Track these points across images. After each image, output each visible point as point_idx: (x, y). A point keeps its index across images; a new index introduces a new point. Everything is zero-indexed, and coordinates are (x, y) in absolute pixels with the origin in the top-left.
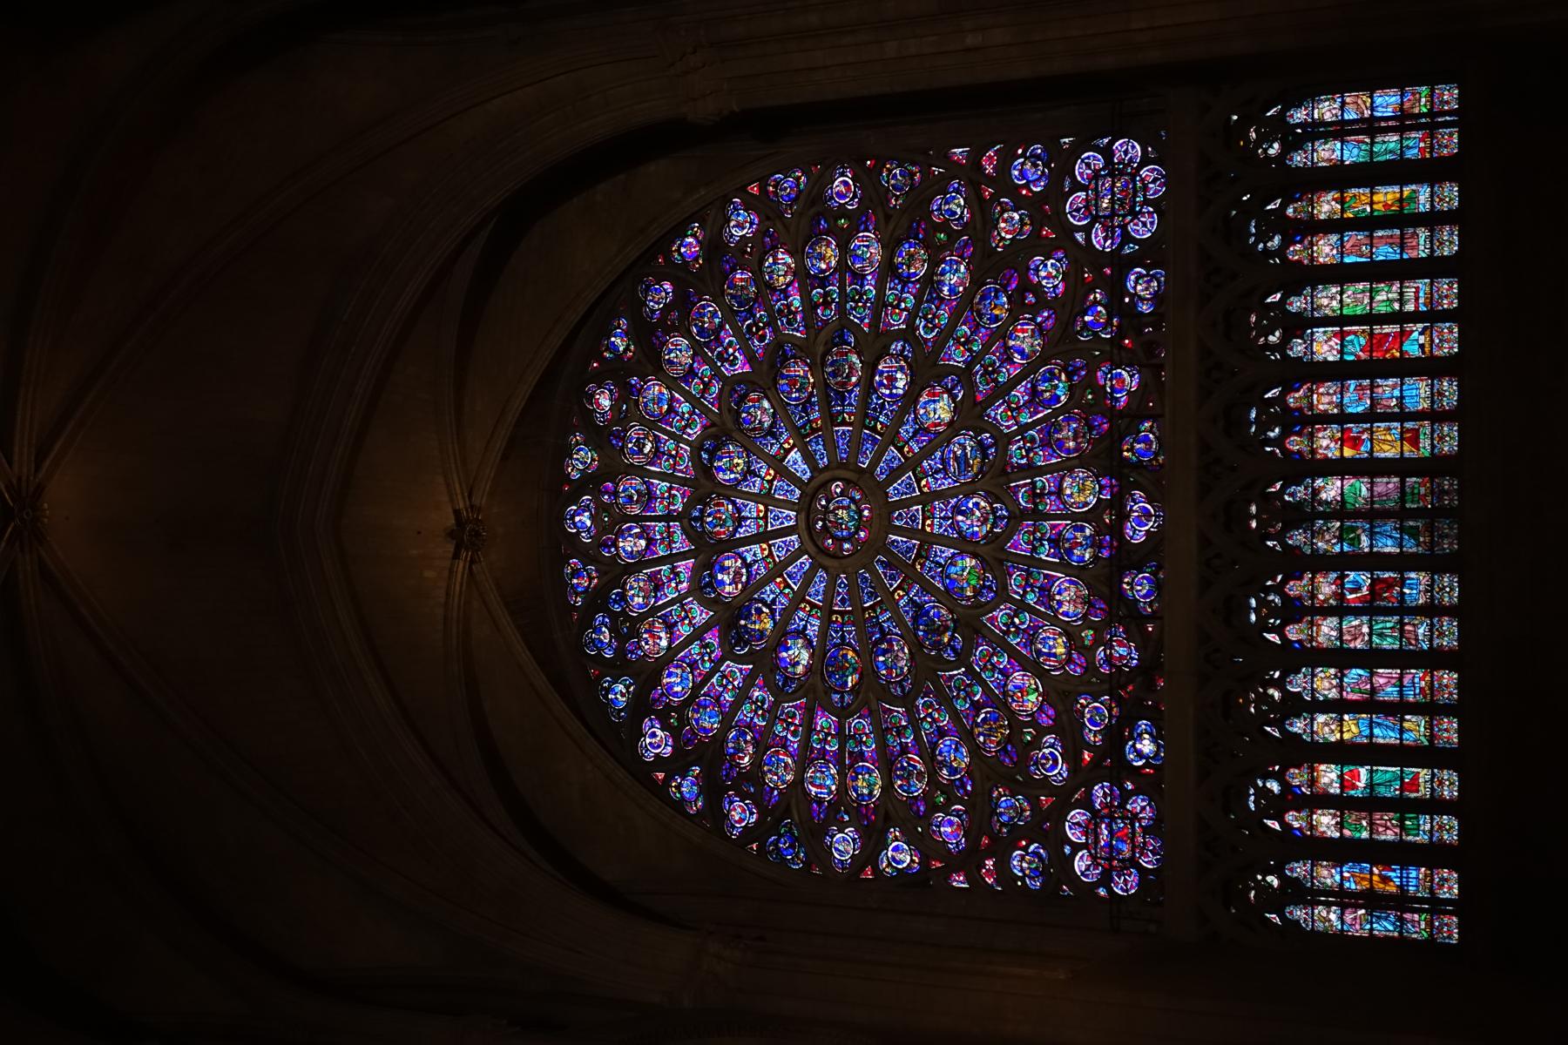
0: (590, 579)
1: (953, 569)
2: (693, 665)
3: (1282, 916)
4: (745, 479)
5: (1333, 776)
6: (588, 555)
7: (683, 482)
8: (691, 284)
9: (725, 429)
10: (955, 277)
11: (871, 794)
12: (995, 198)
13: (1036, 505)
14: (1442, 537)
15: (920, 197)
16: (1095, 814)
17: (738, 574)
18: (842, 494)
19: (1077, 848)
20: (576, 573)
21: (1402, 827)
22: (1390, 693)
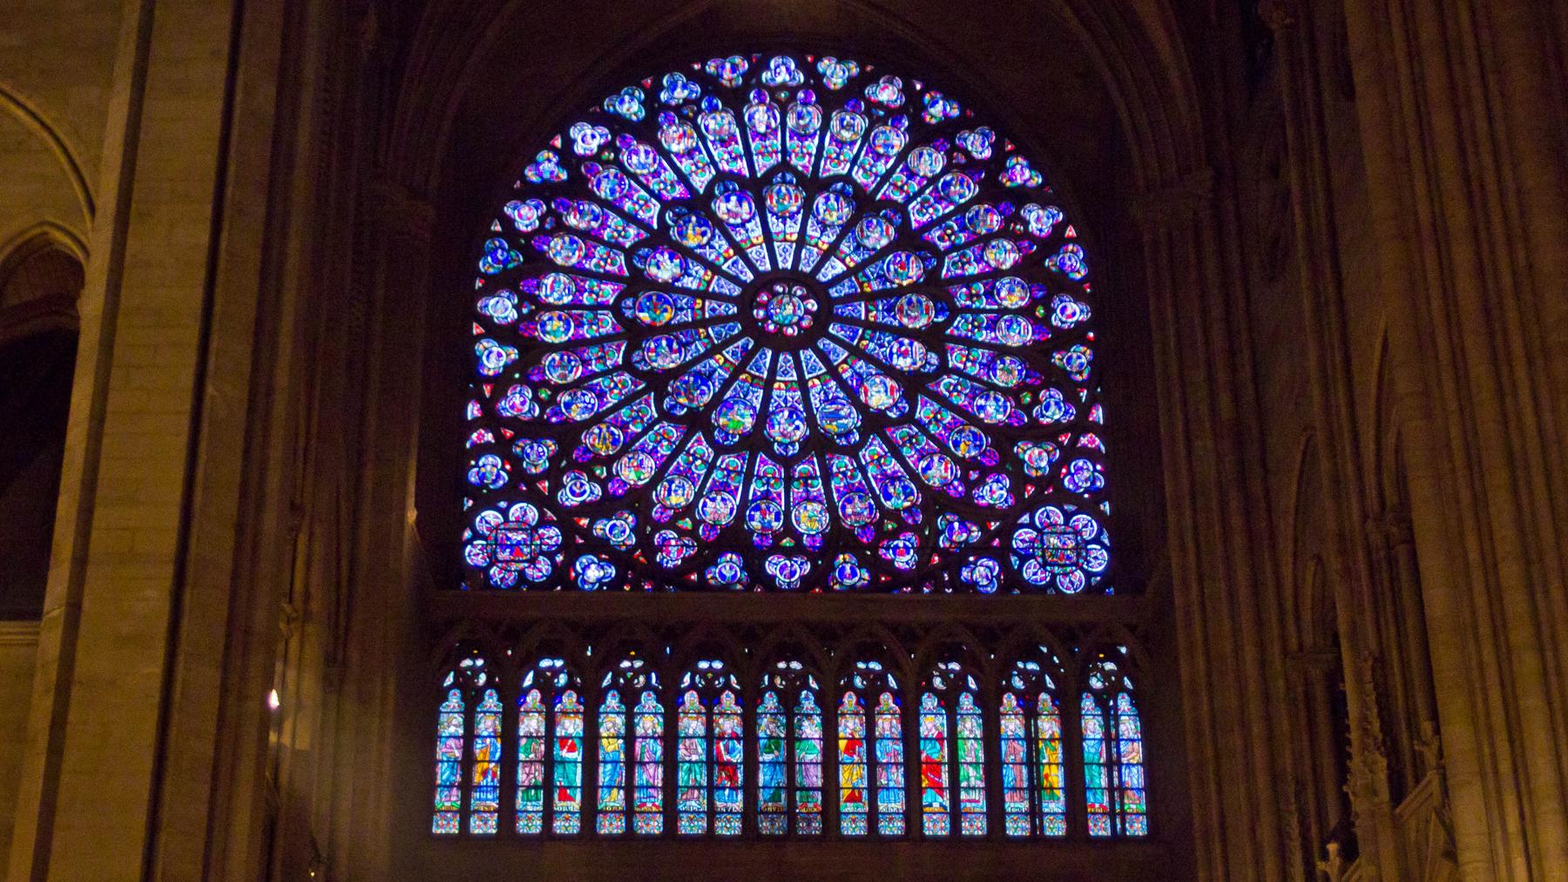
2: (656, 174)
5: (571, 731)
7: (816, 166)
8: (989, 175)
9: (865, 204)
10: (993, 411)
11: (545, 333)
12: (1060, 446)
14: (772, 822)
16: (534, 529)
17: (736, 215)
18: (807, 311)
19: (504, 512)
20: (734, 68)
21: (529, 787)
22: (641, 777)
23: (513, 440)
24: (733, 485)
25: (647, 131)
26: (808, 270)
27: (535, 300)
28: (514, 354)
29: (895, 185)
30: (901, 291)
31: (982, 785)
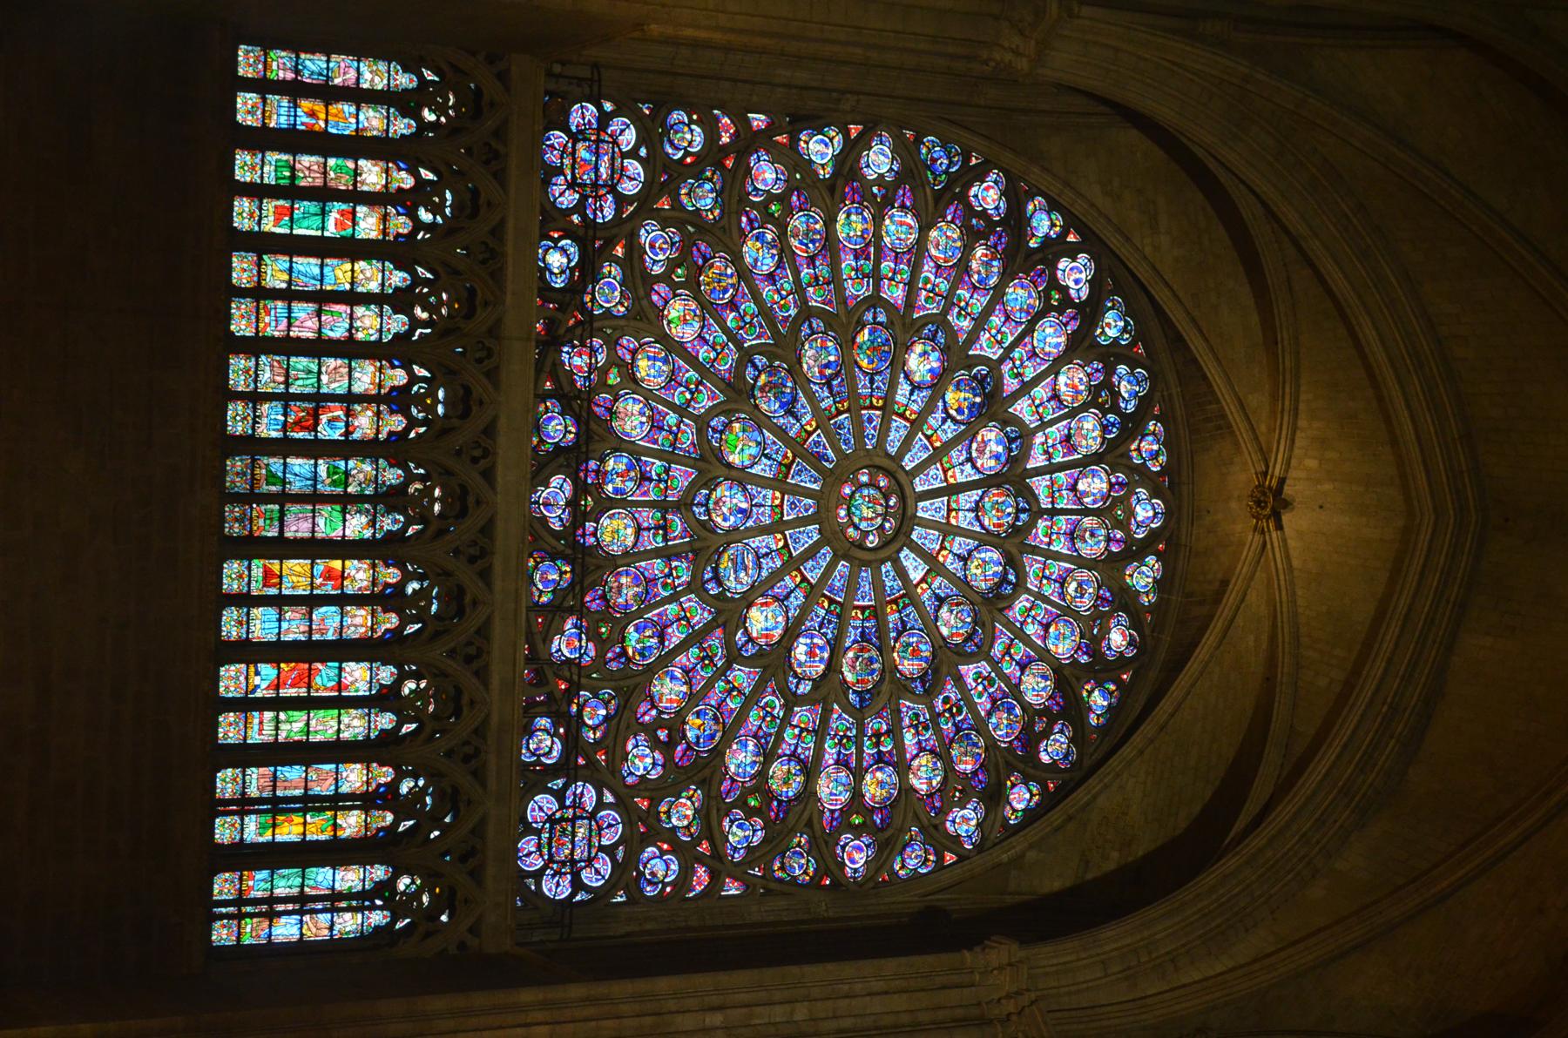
0: (1138, 450)
1: (754, 451)
3: (421, 77)
4: (970, 552)
5: (362, 225)
6: (1140, 474)
7: (1035, 550)
9: (990, 605)
10: (741, 759)
12: (696, 841)
13: (664, 518)
14: (244, 474)
15: (775, 843)
16: (612, 189)
17: (981, 452)
19: (633, 154)
20: (1155, 456)
21: (293, 169)
22: (302, 310)
23: (719, 165)
24: (661, 437)
26: (914, 536)
28: (825, 174)
29: (1009, 647)
31: (281, 739)
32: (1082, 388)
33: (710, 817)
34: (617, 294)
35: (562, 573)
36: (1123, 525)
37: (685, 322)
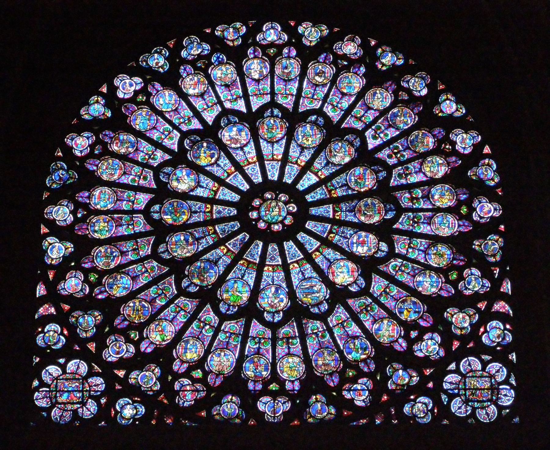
0: (233, 41)
1: (240, 284)
4: (300, 146)
6: (249, 39)
7: (296, 104)
9: (333, 132)
10: (429, 285)
12: (478, 310)
13: (282, 339)
16: (85, 379)
18: (289, 213)
19: (63, 367)
20: (236, 30)
25: (171, 80)
26: (289, 181)
27: (85, 206)
28: (70, 246)
29: (356, 117)
30: (360, 196)
32: (196, 78)
33: (462, 302)
34: (147, 374)
35: (317, 401)
36: (280, 48)
37: (162, 331)
